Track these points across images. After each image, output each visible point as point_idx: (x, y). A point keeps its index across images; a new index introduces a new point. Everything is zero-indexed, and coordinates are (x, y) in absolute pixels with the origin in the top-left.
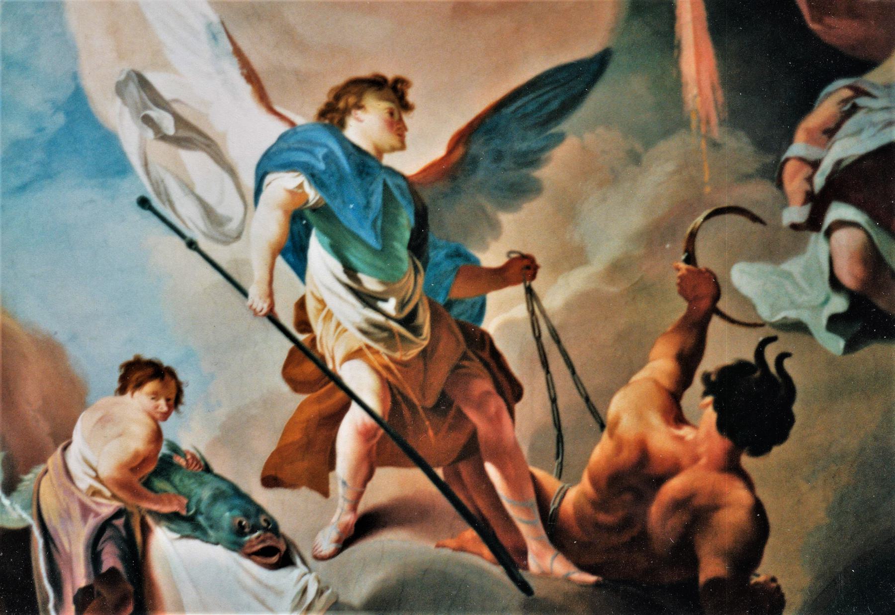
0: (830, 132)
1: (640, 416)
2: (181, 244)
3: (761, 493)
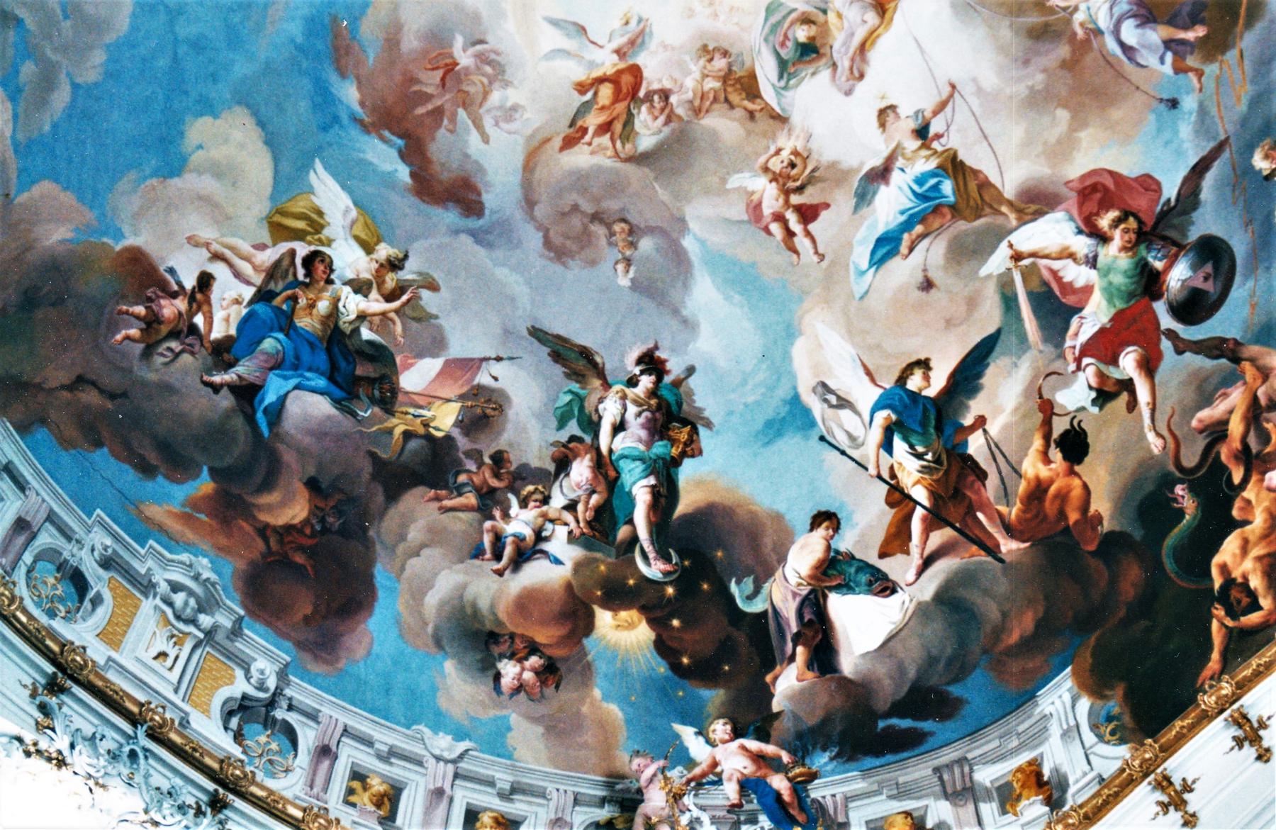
0: (1076, 334)
1: (1034, 466)
2: (837, 453)
3: (1085, 479)
